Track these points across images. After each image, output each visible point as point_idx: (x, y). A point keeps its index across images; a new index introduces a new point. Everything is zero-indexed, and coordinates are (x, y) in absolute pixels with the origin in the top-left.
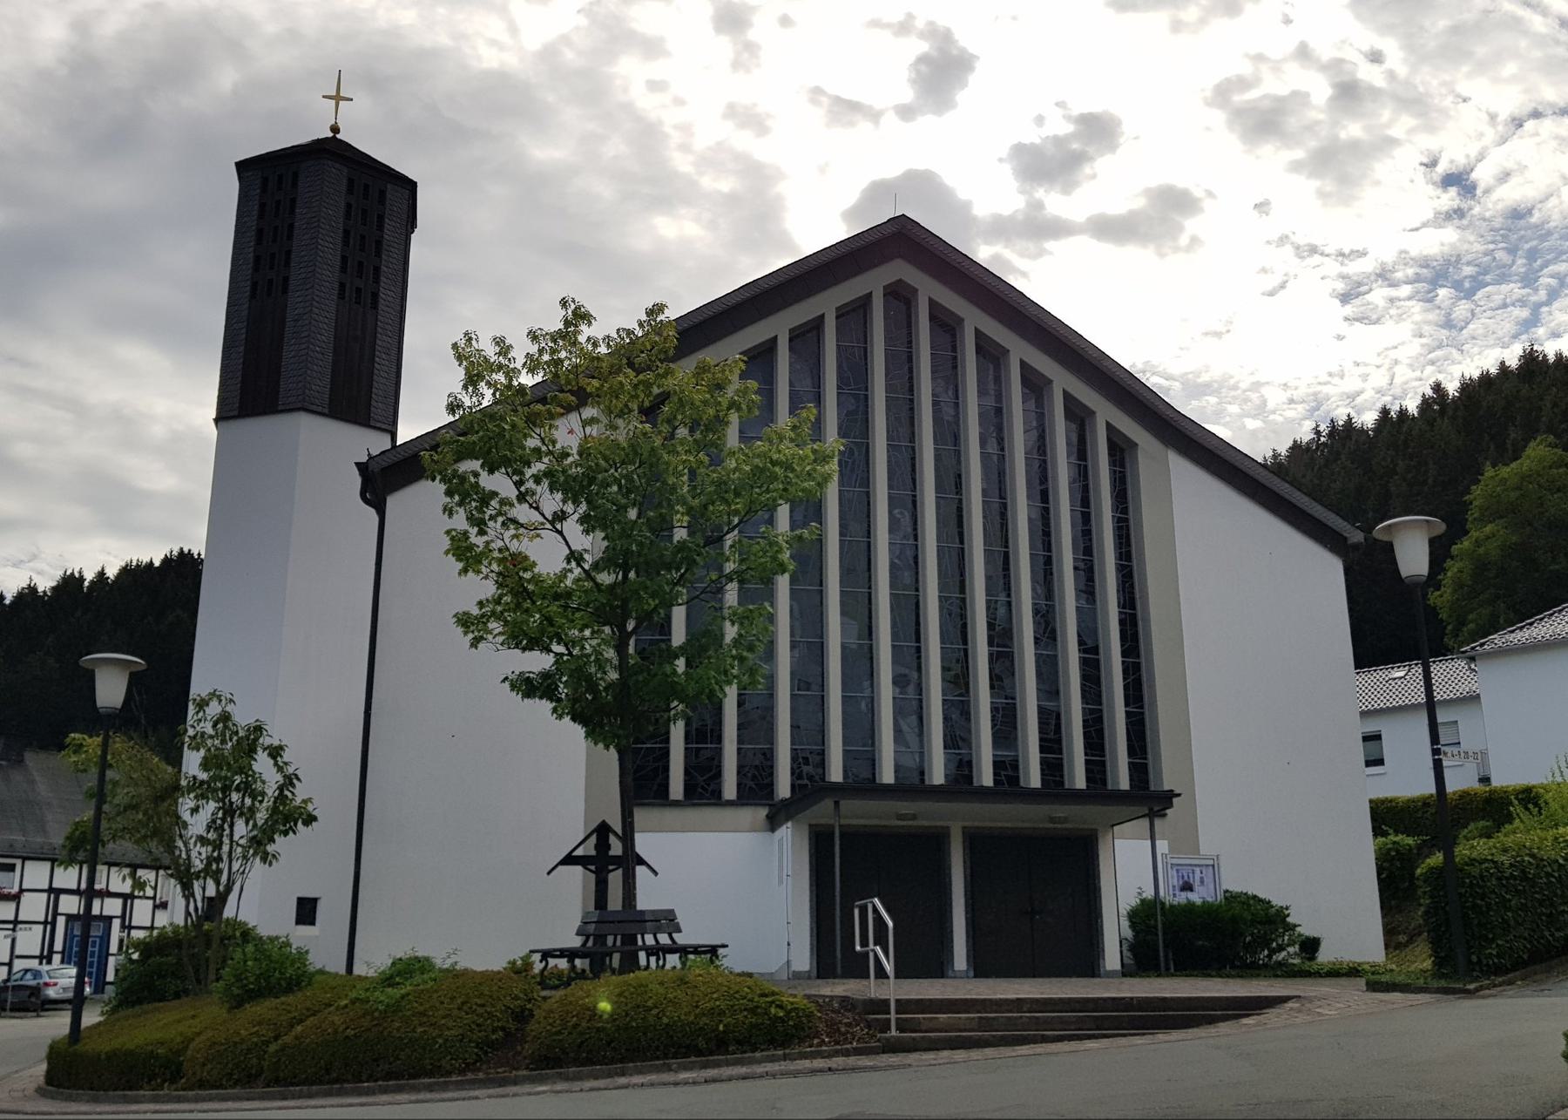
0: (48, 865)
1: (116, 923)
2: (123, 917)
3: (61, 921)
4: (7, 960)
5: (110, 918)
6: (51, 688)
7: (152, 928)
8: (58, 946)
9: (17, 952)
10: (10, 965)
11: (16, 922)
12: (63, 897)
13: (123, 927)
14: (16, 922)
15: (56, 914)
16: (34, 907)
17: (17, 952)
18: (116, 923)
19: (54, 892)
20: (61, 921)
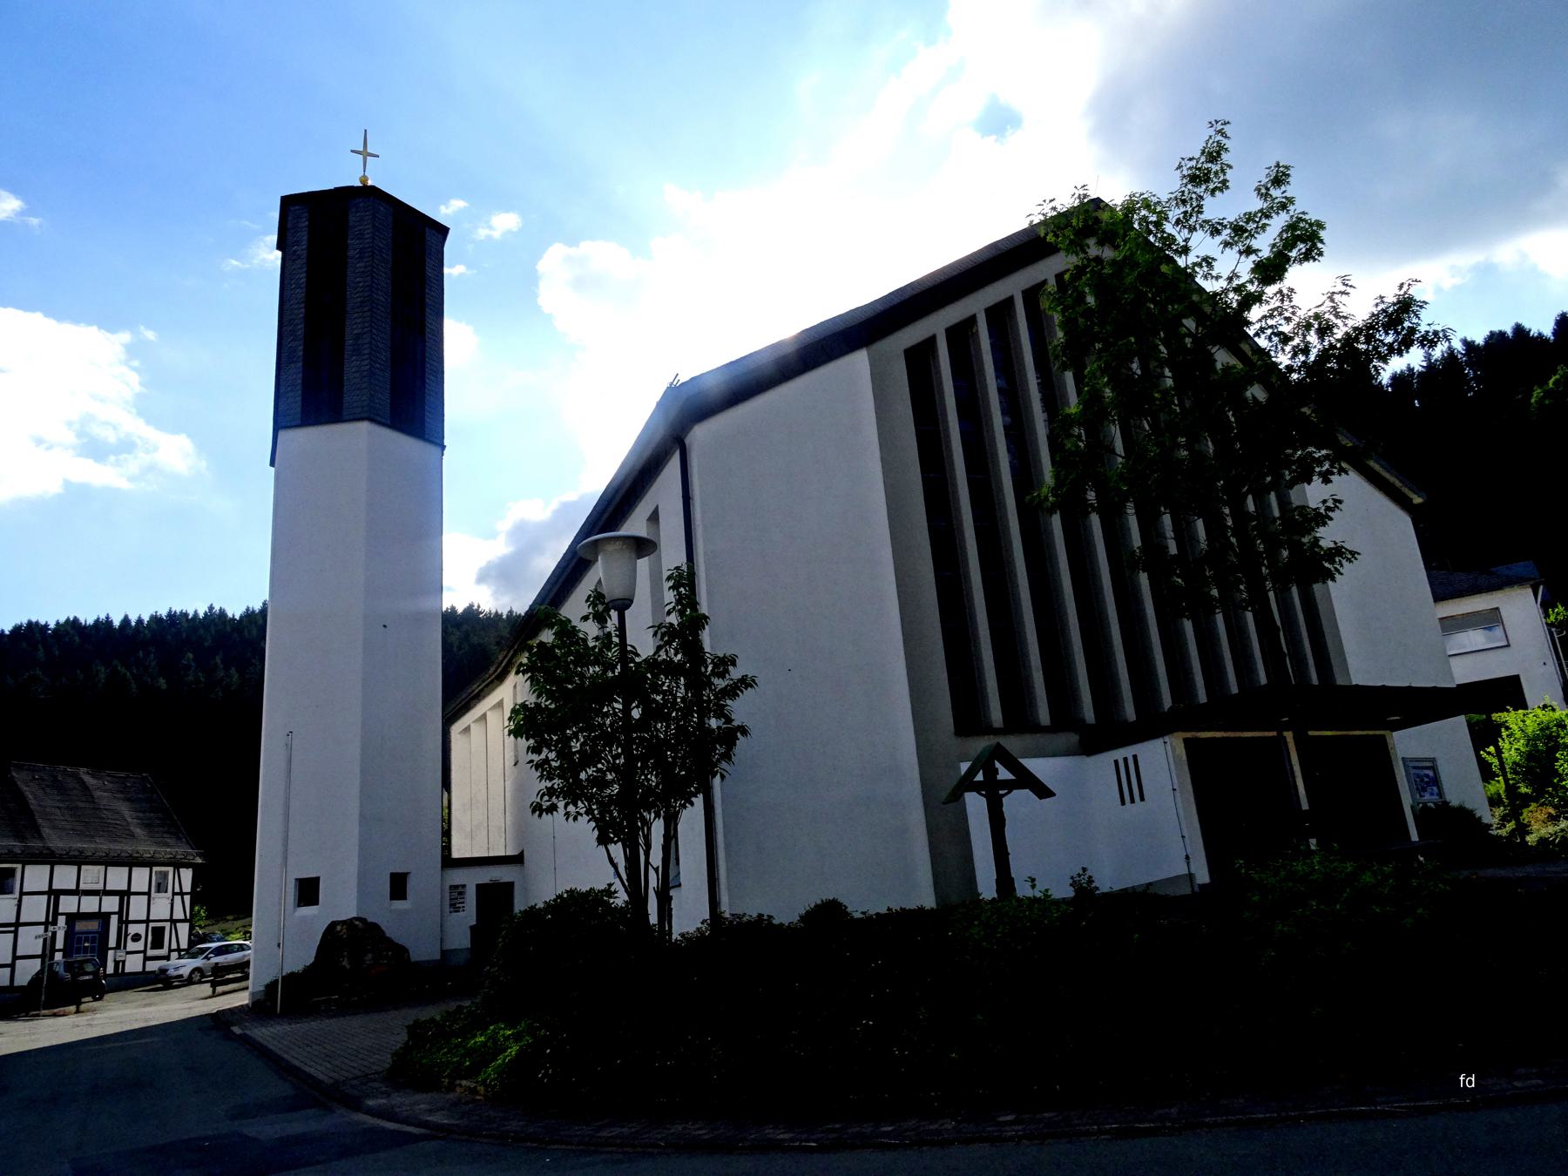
0: (75, 868)
1: (114, 920)
2: (120, 913)
3: (62, 920)
4: (9, 961)
5: (109, 915)
6: (130, 722)
7: (147, 921)
8: (60, 944)
9: (19, 953)
10: (12, 966)
11: (18, 924)
12: (62, 898)
13: (120, 921)
14: (18, 924)
15: (56, 914)
16: (35, 909)
17: (19, 953)
18: (114, 920)
19: (54, 894)
20: (62, 920)
